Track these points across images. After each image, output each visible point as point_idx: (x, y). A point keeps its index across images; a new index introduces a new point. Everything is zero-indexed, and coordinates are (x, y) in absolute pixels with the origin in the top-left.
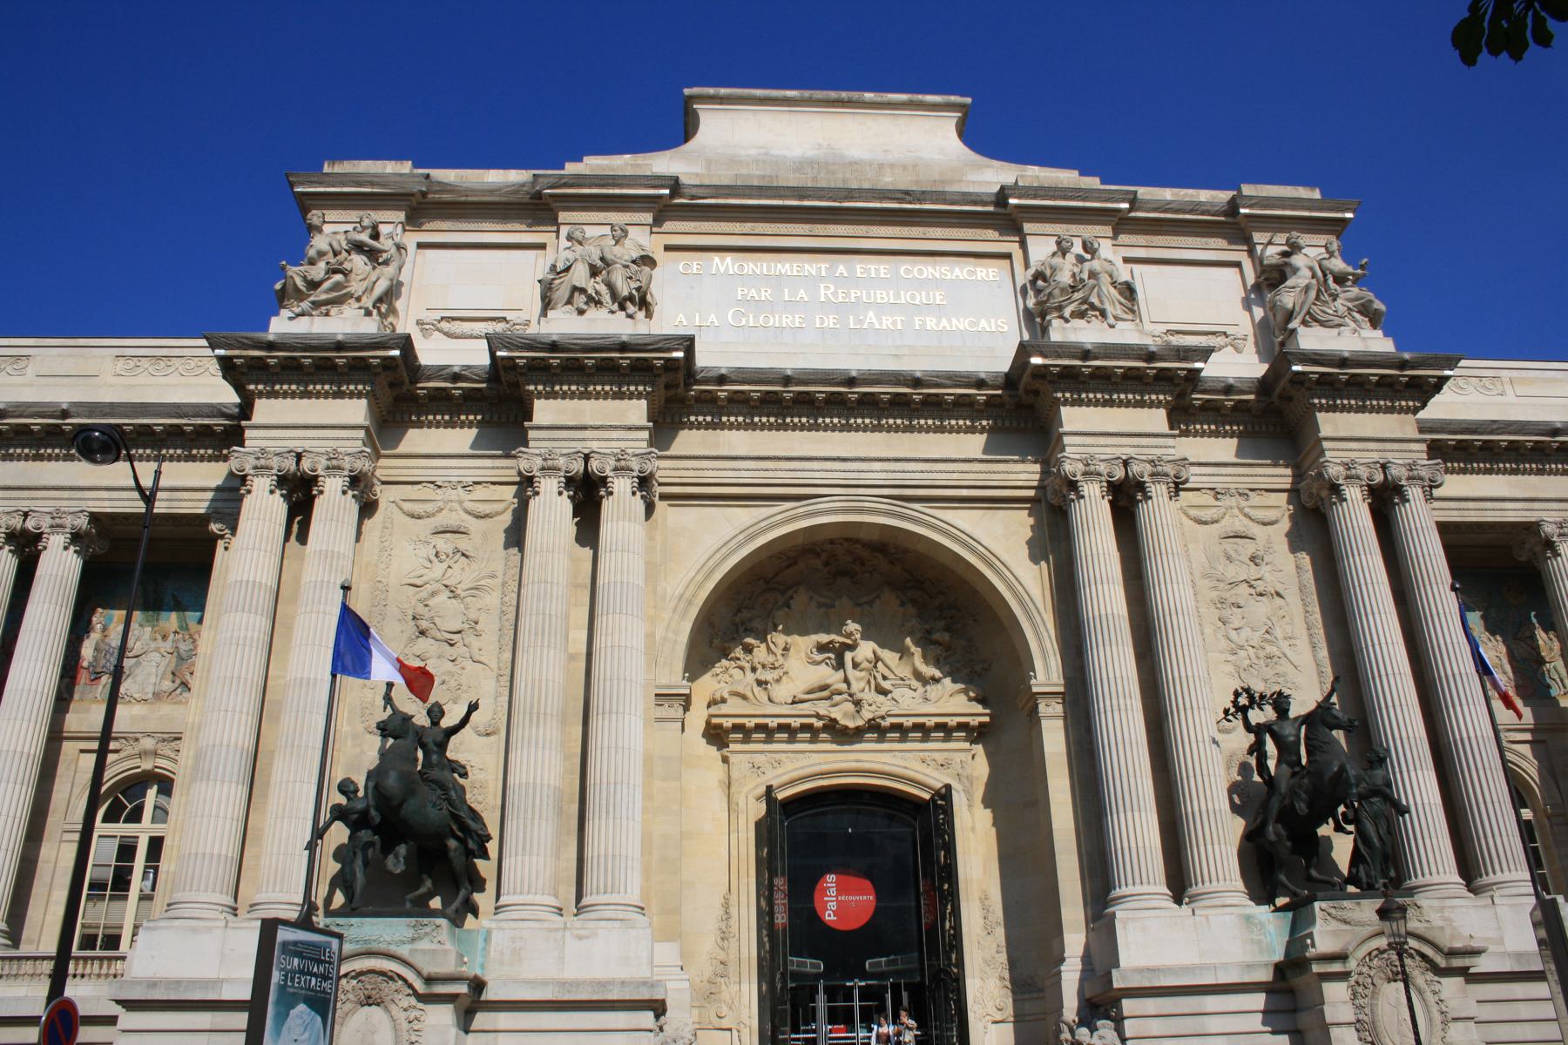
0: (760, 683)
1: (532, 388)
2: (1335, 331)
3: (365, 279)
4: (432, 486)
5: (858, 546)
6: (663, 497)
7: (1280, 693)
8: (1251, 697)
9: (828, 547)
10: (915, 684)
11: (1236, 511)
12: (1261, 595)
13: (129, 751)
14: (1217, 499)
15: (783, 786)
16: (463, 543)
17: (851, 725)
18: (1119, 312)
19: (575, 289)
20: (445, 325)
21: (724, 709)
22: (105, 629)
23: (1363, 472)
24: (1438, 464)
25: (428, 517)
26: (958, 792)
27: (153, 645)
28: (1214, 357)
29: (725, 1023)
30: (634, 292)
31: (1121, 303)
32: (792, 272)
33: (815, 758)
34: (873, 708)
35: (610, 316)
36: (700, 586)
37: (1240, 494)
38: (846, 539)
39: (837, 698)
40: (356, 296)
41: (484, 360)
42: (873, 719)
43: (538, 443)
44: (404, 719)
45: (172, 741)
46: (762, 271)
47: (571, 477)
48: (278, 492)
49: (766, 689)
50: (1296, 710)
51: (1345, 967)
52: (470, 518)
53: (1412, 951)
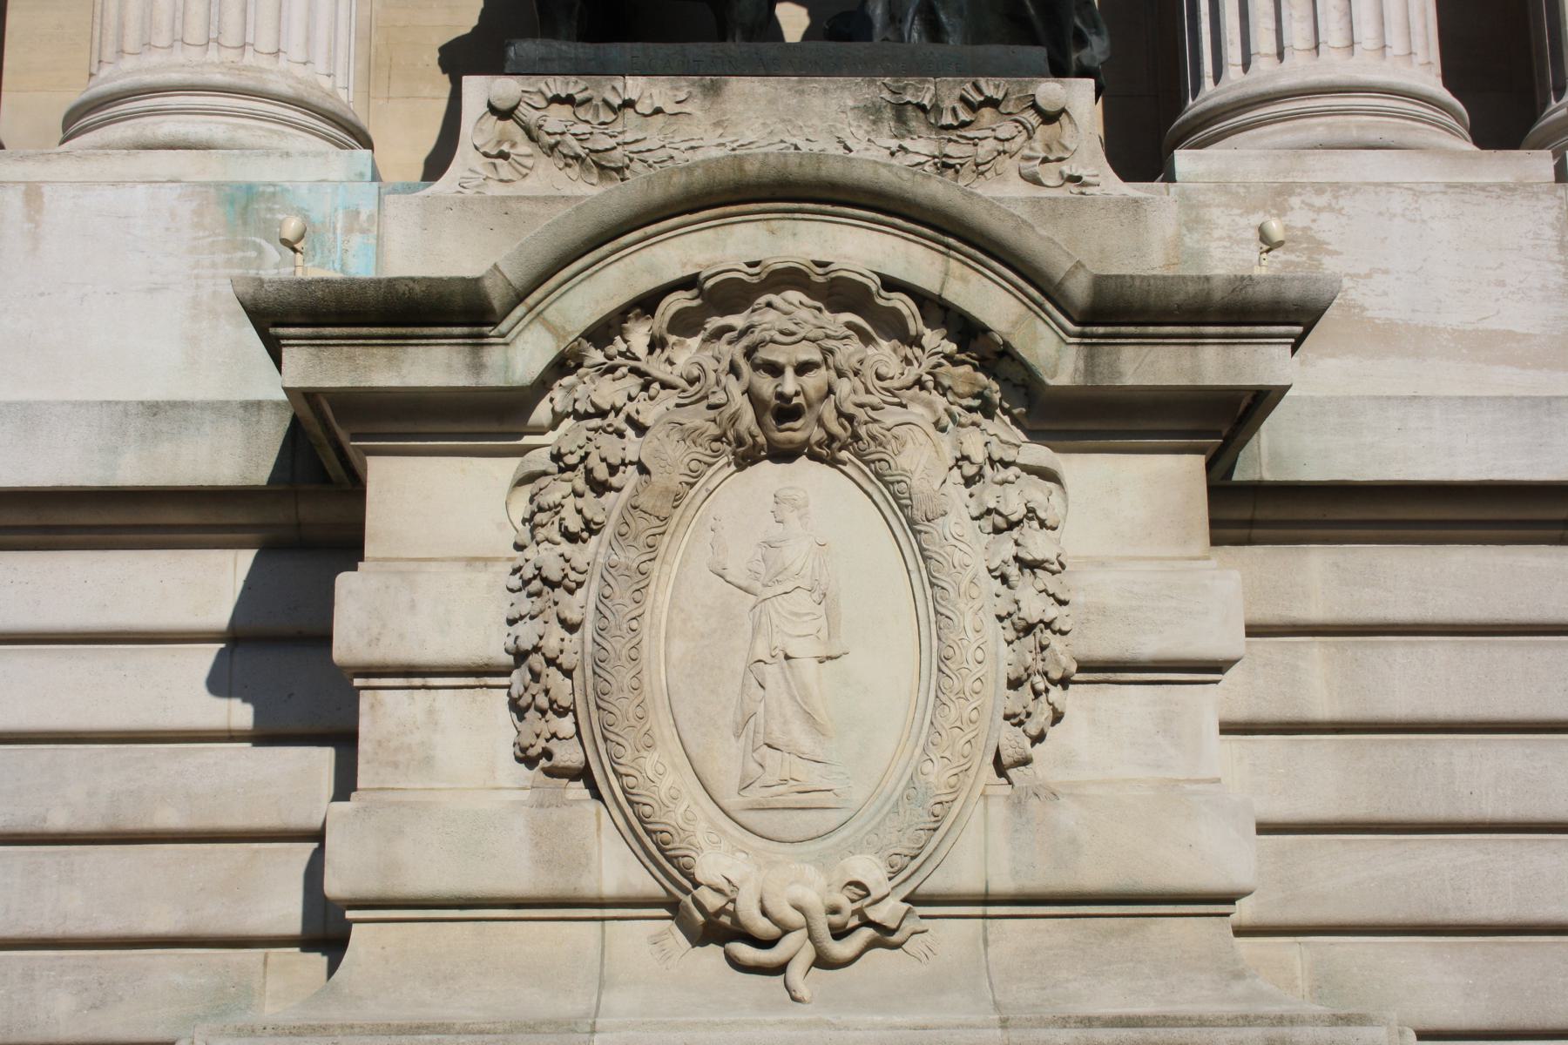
51: (477, 367)
53: (902, 303)
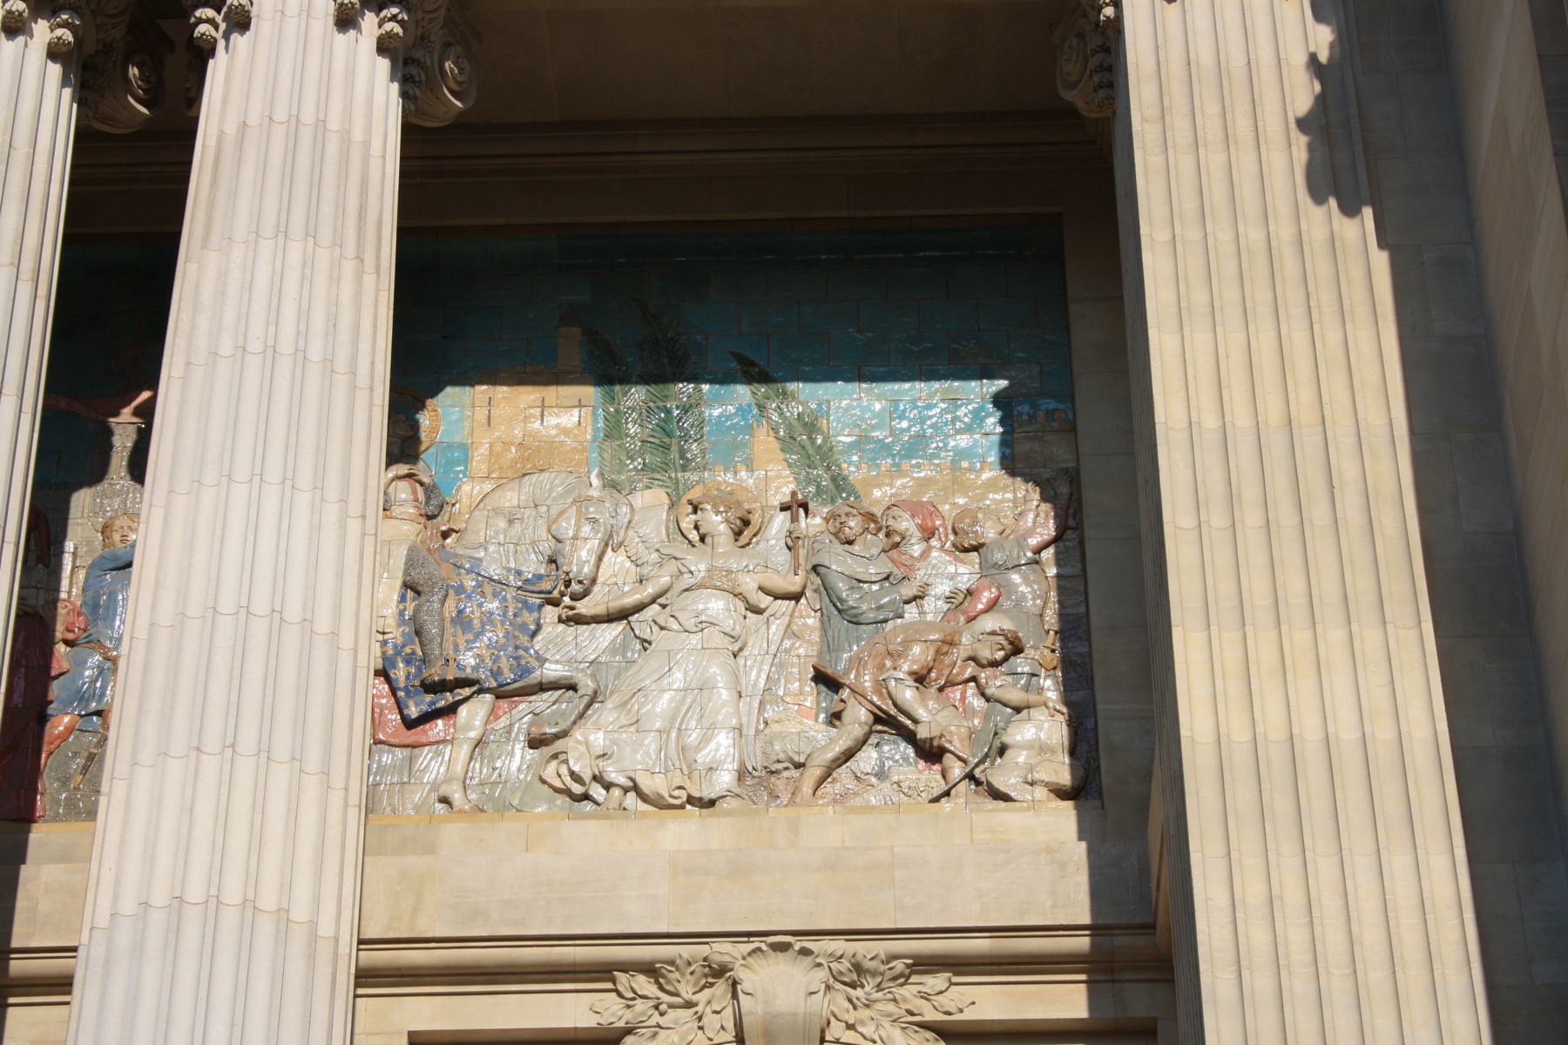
45: (903, 978)
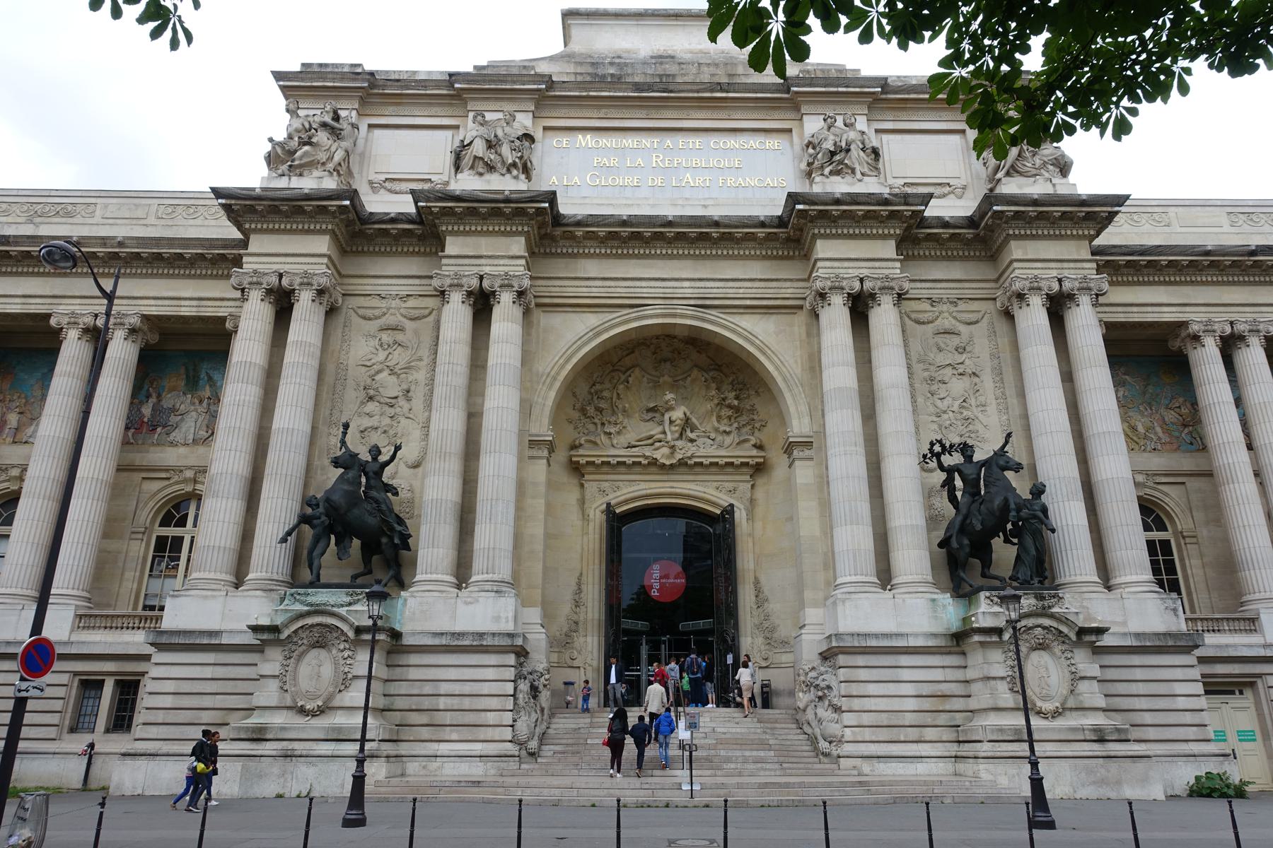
0: (606, 433)
1: (444, 228)
2: (1033, 179)
3: (328, 149)
4: (378, 297)
5: (675, 340)
6: (538, 305)
7: (965, 444)
8: (943, 446)
9: (654, 341)
10: (713, 435)
11: (946, 315)
12: (961, 374)
13: (176, 478)
14: (932, 306)
15: (620, 504)
16: (400, 337)
17: (668, 463)
18: (866, 170)
19: (476, 157)
20: (387, 185)
21: (581, 452)
22: (159, 396)
23: (1044, 284)
24: (1103, 278)
25: (376, 319)
26: (740, 509)
27: (193, 408)
28: (933, 202)
29: (576, 663)
30: (517, 160)
31: (868, 163)
32: (633, 145)
33: (643, 485)
34: (683, 451)
35: (502, 177)
36: (563, 367)
37: (951, 303)
38: (668, 336)
39: (658, 444)
40: (322, 161)
41: (411, 209)
42: (682, 459)
43: (449, 268)
44: (351, 455)
46: (611, 145)
47: (471, 291)
48: (267, 300)
49: (610, 438)
50: (978, 456)
52: (404, 320)
53: (1052, 629)
